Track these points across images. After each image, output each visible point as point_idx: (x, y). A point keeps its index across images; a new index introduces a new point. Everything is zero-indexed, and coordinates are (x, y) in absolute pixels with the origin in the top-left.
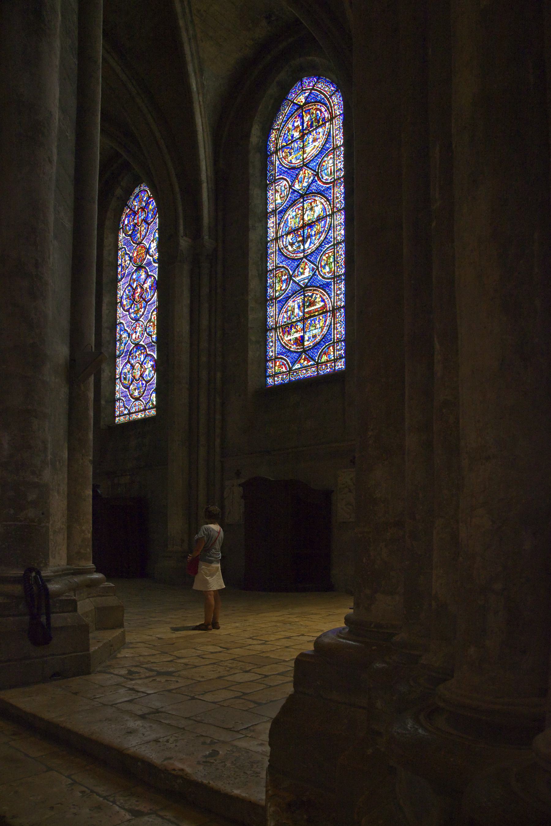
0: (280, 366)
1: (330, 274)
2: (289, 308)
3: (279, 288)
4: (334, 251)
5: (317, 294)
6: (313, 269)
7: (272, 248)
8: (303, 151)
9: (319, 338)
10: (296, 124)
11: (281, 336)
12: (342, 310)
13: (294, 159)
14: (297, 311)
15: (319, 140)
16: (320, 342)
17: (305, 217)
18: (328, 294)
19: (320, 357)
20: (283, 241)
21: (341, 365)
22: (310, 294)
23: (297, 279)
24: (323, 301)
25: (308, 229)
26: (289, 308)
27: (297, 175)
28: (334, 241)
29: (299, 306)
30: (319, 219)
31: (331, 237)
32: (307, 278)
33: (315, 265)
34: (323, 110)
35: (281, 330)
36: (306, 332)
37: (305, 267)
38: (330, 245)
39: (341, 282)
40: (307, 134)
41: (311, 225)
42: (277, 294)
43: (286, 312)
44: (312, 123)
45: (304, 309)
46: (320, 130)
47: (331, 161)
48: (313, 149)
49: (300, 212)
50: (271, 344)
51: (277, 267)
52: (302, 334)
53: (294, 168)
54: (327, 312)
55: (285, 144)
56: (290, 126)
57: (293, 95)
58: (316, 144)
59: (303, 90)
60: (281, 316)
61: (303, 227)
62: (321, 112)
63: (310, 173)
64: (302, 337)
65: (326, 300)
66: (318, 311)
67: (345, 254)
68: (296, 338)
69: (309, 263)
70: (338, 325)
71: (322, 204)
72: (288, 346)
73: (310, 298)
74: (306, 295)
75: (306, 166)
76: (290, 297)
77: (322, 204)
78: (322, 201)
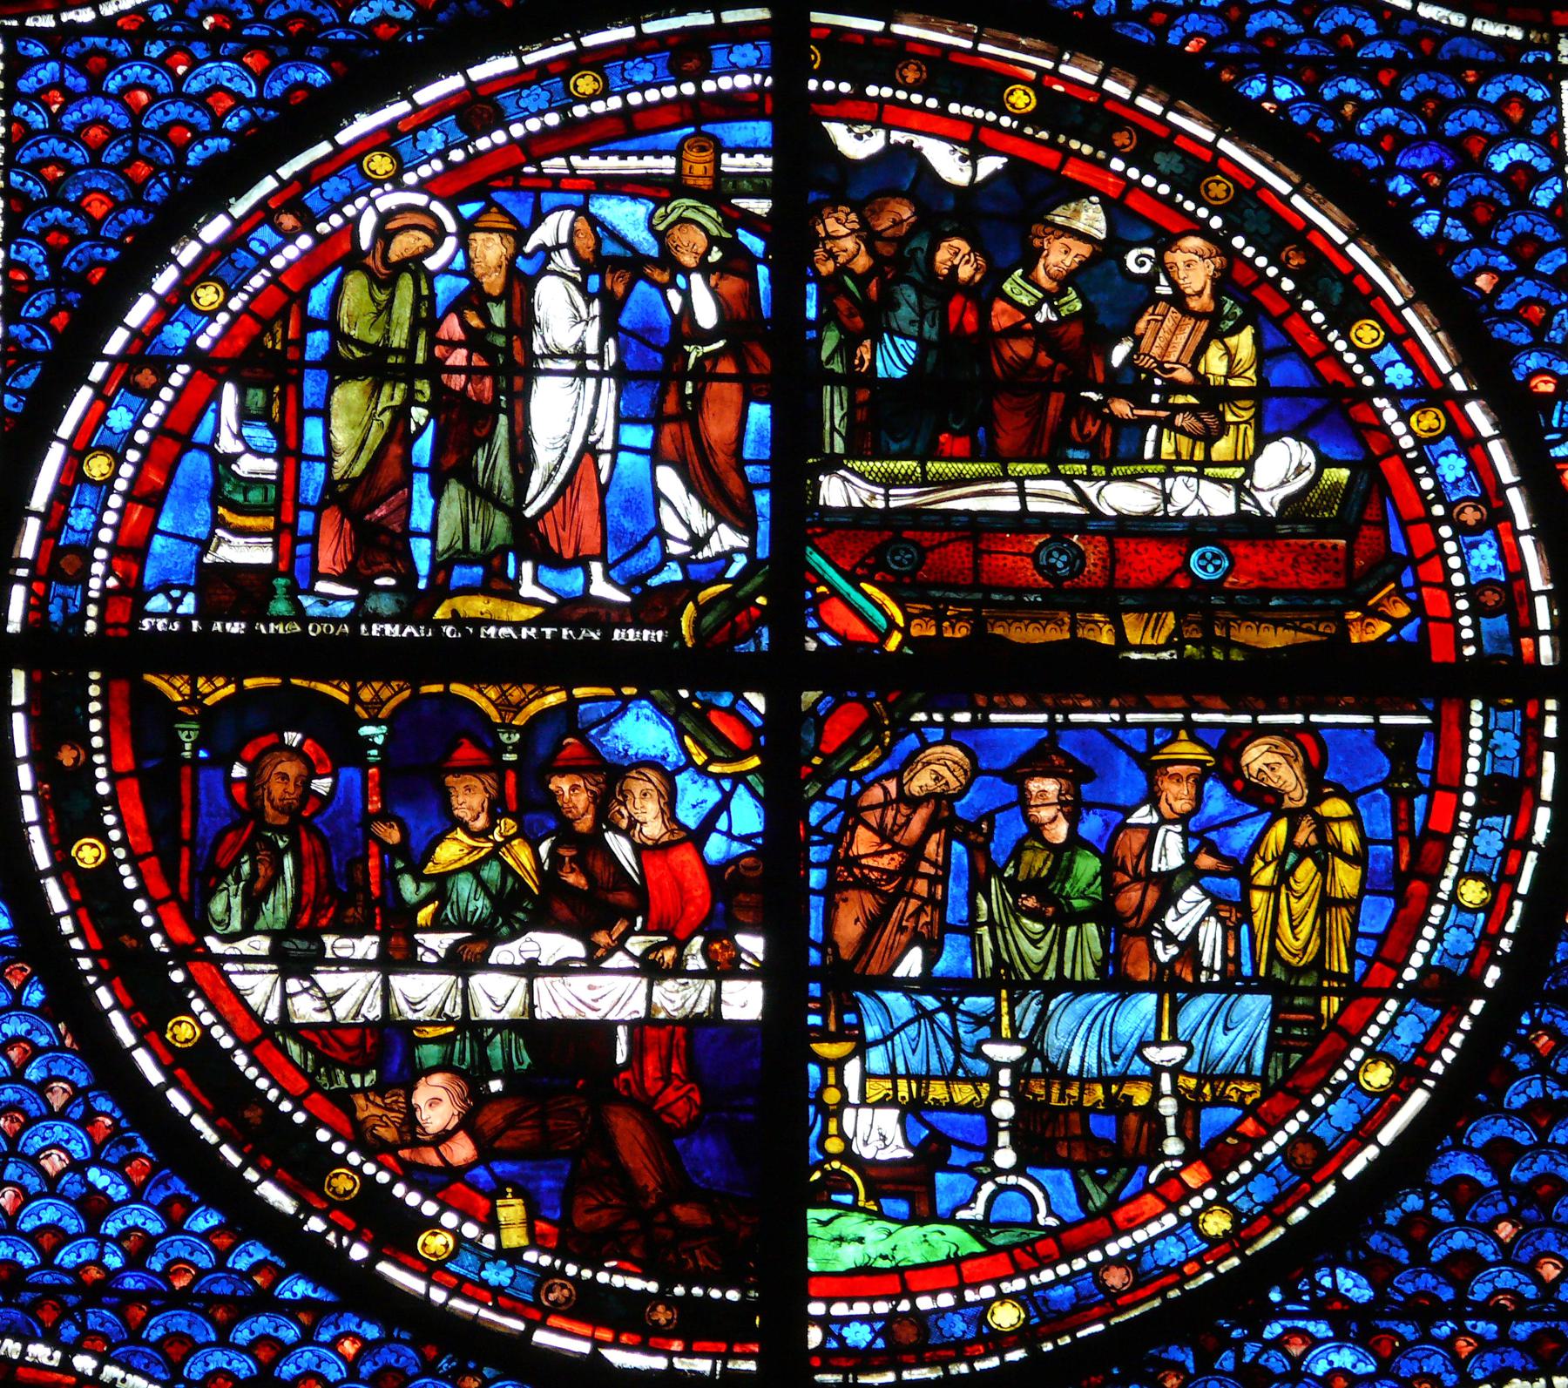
16: (1241, 1299)
36: (853, 978)
45: (798, 454)
52: (744, 1001)
72: (306, 1170)
73: (956, 257)
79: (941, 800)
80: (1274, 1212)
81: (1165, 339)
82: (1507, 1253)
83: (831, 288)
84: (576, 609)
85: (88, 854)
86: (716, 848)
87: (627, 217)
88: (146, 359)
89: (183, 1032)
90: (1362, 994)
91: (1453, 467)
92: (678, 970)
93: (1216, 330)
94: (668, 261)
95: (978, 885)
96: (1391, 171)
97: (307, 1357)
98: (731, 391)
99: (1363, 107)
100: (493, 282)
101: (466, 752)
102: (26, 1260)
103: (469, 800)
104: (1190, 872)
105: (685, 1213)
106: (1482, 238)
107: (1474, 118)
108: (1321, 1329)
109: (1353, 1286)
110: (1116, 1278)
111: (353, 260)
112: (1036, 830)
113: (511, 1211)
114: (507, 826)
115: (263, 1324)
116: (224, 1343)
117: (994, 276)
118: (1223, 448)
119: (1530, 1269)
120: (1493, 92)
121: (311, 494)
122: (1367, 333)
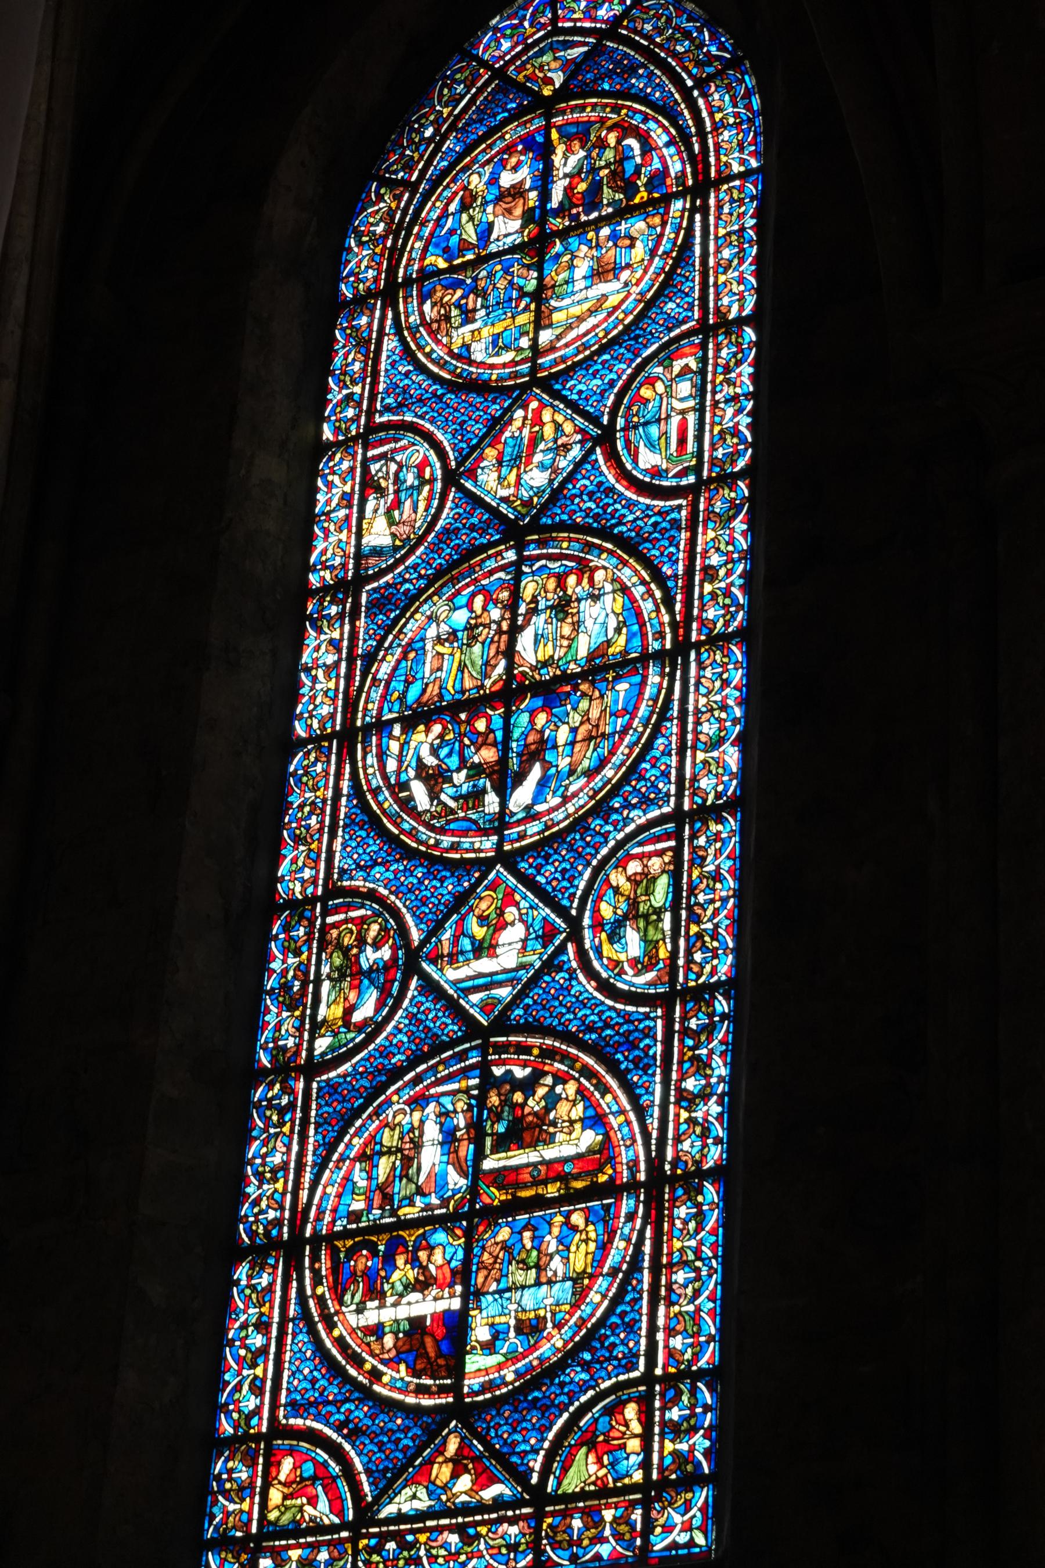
0: (298, 1487)
1: (650, 976)
2: (388, 1138)
3: (338, 1011)
4: (678, 851)
5: (561, 1079)
6: (548, 934)
7: (314, 784)
8: (538, 313)
9: (553, 1344)
10: (507, 179)
11: (321, 1300)
12: (710, 1193)
13: (485, 341)
14: (431, 1157)
15: (625, 275)
16: (561, 1366)
17: (525, 642)
18: (629, 1088)
19: (559, 1455)
20: (382, 756)
22: (520, 1073)
23: (449, 976)
24: (597, 1120)
25: (533, 714)
26: (388, 1138)
27: (496, 425)
28: (680, 796)
29: (449, 1138)
30: (606, 668)
31: (665, 774)
32: (509, 977)
33: (562, 911)
34: (660, 138)
35: (324, 1265)
36: (479, 1294)
37: (501, 912)
38: (654, 813)
39: (709, 1029)
40: (564, 234)
41: (552, 689)
42: (322, 1044)
43: (367, 1158)
44: (596, 188)
45: (480, 1155)
46: (637, 226)
47: (684, 388)
48: (591, 312)
49: (495, 613)
50: (257, 1340)
51: (333, 891)
52: (456, 1304)
53: (482, 387)
54: (614, 1189)
55: (442, 264)
56: (476, 182)
57: (506, 45)
58: (612, 289)
59: (557, 31)
60: (332, 1176)
61: (510, 693)
62: (648, 147)
63: (568, 428)
64: (456, 1326)
65: (615, 1121)
66: (564, 1178)
67: (741, 874)
68: (416, 1323)
69: (526, 899)
70: (680, 1277)
71: (625, 590)
73: (518, 1097)
74: (498, 1071)
75: (545, 384)
76: (396, 1073)
77: (625, 590)
78: (626, 574)
79: (504, 1242)
80: (572, 1339)
81: (563, 1108)
82: (622, 1342)
83: (490, 1110)
84: (428, 1207)
85: (320, 1290)
86: (454, 1264)
87: (446, 1101)
88: (342, 1159)
89: (336, 1333)
90: (593, 1277)
91: (626, 1130)
92: (442, 1298)
93: (574, 1103)
94: (455, 1112)
95: (510, 1263)
96: (616, 1053)
97: (356, 1414)
98: (466, 1143)
99: (611, 1037)
100: (416, 1124)
101: (401, 1249)
102: (298, 1398)
103: (400, 1261)
104: (558, 1252)
105: (441, 1362)
106: (637, 1067)
107: (636, 1034)
108: (578, 1369)
109: (587, 1356)
110: (535, 1363)
111: (387, 1125)
112: (524, 1246)
113: (403, 1367)
114: (408, 1266)
115: (347, 1406)
116: (339, 1412)
117: (526, 1099)
118: (574, 1136)
119: (627, 1345)
120: (641, 1026)
121: (373, 1188)
122: (609, 1098)
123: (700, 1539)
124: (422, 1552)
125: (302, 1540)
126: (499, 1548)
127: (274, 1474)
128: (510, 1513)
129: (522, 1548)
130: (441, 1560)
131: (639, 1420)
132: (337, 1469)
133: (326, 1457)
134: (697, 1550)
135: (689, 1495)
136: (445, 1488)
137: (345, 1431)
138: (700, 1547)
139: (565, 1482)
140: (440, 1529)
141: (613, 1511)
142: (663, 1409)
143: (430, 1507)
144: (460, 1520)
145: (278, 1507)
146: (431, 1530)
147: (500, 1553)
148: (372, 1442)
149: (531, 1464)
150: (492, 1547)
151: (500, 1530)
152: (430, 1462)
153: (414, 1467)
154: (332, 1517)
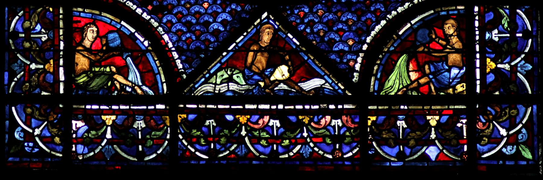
0: (102, 55)
19: (380, 59)
21: (512, 140)
123: (528, 155)
124: (243, 133)
125: (114, 107)
126: (324, 137)
127: (78, 39)
128: (332, 107)
129: (348, 140)
130: (263, 142)
131: (459, 36)
132: (146, 43)
133: (133, 30)
134: (524, 163)
135: (514, 112)
136: (262, 75)
137: (150, 8)
138: (527, 160)
139: (388, 84)
140: (262, 113)
141: (437, 118)
142: (483, 29)
143: (247, 91)
144: (281, 107)
145: (84, 72)
146: (251, 112)
147: (324, 142)
148: (179, 21)
149: (351, 63)
150: (316, 136)
151: (323, 122)
152: (244, 49)
153: (228, 52)
154: (144, 88)
